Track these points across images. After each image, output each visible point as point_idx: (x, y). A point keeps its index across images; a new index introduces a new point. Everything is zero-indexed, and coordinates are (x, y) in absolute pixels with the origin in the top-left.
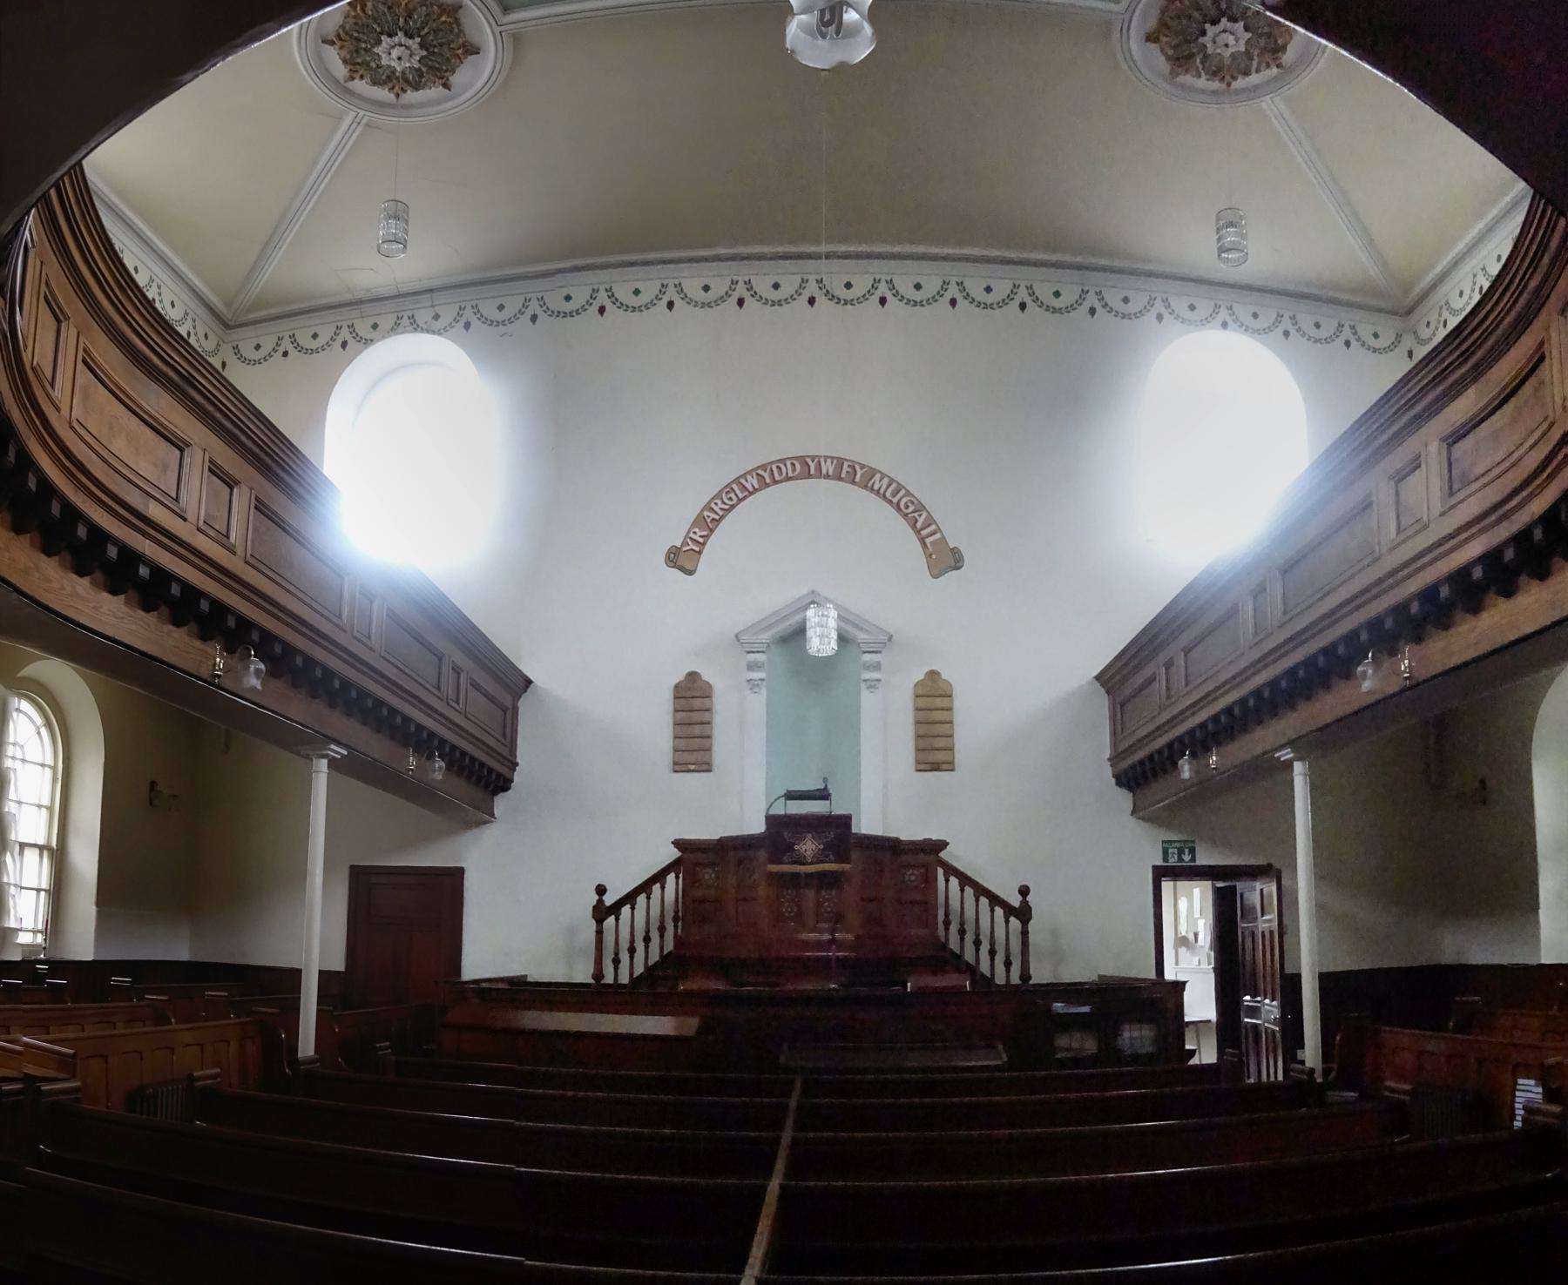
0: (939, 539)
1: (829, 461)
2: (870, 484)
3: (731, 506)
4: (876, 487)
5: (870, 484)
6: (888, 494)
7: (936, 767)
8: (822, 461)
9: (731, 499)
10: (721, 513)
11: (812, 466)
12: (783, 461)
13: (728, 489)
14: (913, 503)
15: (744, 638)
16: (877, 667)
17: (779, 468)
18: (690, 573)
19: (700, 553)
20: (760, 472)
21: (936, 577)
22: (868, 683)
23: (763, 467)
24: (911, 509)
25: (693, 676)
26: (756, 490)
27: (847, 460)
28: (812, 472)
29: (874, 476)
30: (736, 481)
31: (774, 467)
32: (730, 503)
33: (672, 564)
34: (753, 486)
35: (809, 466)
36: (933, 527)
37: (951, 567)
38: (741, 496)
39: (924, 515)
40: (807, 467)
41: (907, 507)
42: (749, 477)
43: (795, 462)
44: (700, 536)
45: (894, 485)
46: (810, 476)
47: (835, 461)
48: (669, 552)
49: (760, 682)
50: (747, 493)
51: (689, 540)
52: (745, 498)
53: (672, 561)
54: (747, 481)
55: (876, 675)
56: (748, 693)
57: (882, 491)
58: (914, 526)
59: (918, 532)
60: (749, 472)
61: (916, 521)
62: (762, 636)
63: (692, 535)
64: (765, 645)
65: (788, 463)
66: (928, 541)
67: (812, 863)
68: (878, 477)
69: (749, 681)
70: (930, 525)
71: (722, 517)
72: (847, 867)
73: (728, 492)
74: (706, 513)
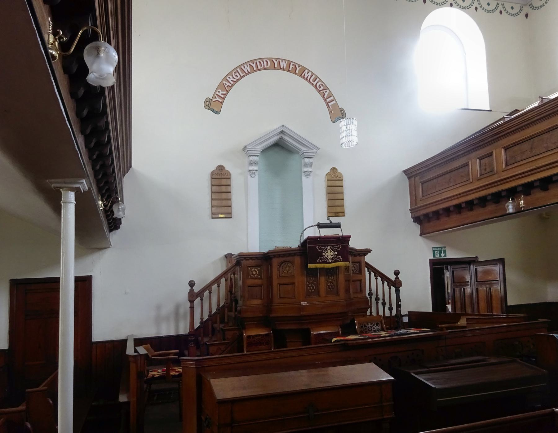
0: (335, 103)
1: (284, 61)
2: (303, 75)
3: (237, 80)
4: (306, 77)
5: (303, 75)
6: (311, 80)
8: (281, 61)
9: (237, 76)
10: (232, 83)
11: (276, 63)
13: (235, 70)
14: (323, 85)
15: (250, 148)
16: (311, 165)
18: (218, 113)
19: (222, 103)
20: (251, 63)
21: (334, 122)
22: (306, 173)
23: (253, 61)
24: (322, 88)
25: (221, 168)
26: (249, 73)
28: (276, 66)
32: (237, 78)
33: (208, 108)
36: (332, 98)
37: (340, 117)
38: (242, 75)
39: (328, 91)
41: (320, 87)
42: (245, 66)
44: (222, 94)
45: (314, 76)
46: (275, 68)
48: (206, 101)
49: (255, 171)
50: (245, 74)
52: (244, 76)
53: (208, 106)
54: (244, 67)
56: (249, 177)
57: (308, 79)
58: (323, 97)
59: (325, 100)
61: (324, 94)
62: (258, 147)
63: (217, 93)
64: (260, 152)
65: (264, 60)
66: (330, 104)
67: (331, 263)
68: (306, 71)
69: (250, 171)
70: (331, 97)
71: (233, 85)
72: (347, 263)
74: (224, 82)
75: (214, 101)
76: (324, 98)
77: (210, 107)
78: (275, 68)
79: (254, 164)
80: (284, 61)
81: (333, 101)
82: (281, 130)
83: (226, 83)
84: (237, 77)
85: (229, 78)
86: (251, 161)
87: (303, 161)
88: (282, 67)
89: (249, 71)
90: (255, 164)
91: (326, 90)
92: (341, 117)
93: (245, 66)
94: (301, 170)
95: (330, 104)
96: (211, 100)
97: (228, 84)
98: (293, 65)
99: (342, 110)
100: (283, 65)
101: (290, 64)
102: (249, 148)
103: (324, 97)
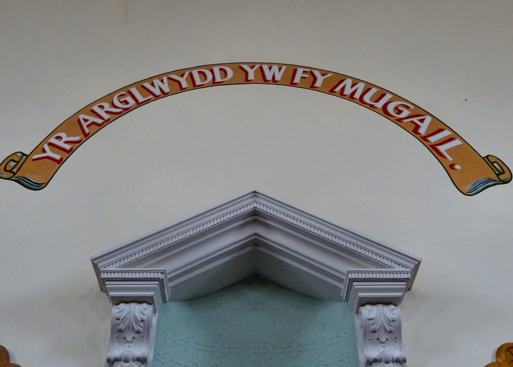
2: (338, 89)
3: (125, 109)
4: (348, 91)
5: (338, 89)
6: (367, 98)
8: (266, 68)
10: (106, 116)
14: (407, 107)
18: (37, 187)
19: (60, 162)
24: (405, 113)
36: (446, 133)
37: (490, 180)
39: (428, 119)
40: (244, 73)
42: (157, 82)
44: (66, 142)
45: (373, 91)
47: (284, 68)
50: (152, 96)
53: (10, 171)
54: (153, 85)
57: (357, 96)
60: (160, 77)
61: (417, 127)
63: (53, 140)
65: (216, 70)
68: (348, 82)
71: (107, 122)
74: (82, 117)
75: (34, 160)
76: (418, 136)
77: (14, 174)
79: (133, 335)
81: (451, 139)
82: (250, 208)
83: (86, 117)
86: (118, 319)
87: (357, 322)
90: (138, 332)
94: (356, 358)
95: (442, 148)
97: (92, 119)
98: (304, 72)
101: (295, 71)
102: (111, 268)
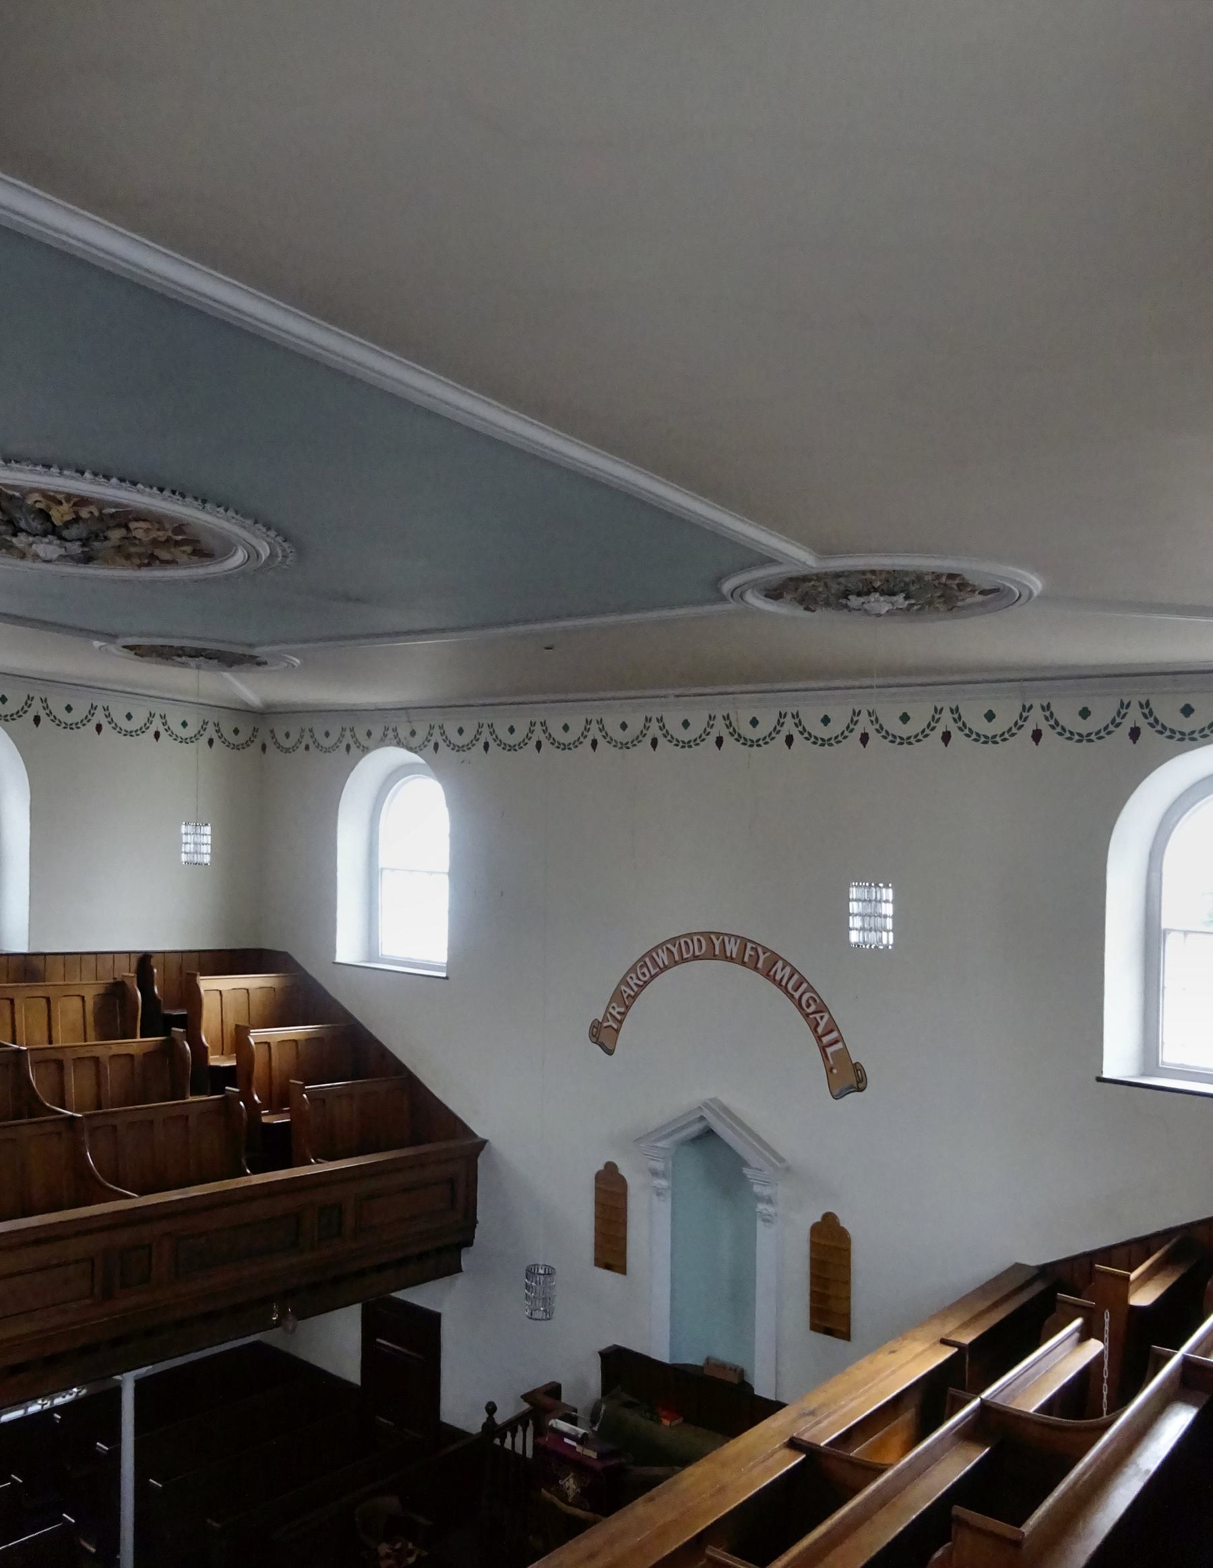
1: (733, 940)
3: (645, 982)
4: (778, 977)
5: (772, 973)
7: (828, 1332)
8: (726, 939)
10: (635, 989)
11: (717, 943)
12: (690, 935)
14: (815, 1001)
16: (769, 1201)
17: (686, 943)
19: (617, 1031)
20: (669, 946)
23: (673, 940)
26: (666, 968)
27: (750, 941)
28: (717, 952)
29: (777, 962)
30: (649, 954)
31: (682, 941)
33: (594, 1040)
34: (663, 962)
35: (714, 945)
36: (834, 1035)
39: (826, 1016)
41: (809, 1006)
42: (660, 951)
43: (702, 939)
45: (796, 977)
46: (715, 957)
47: (738, 941)
48: (593, 1027)
50: (658, 969)
51: (608, 1015)
52: (656, 975)
53: (595, 1036)
55: (771, 1210)
56: (655, 1198)
57: (784, 983)
58: (815, 1030)
59: (819, 1038)
61: (818, 1024)
65: (695, 938)
66: (829, 1050)
68: (780, 964)
70: (831, 1031)
71: (637, 994)
73: (641, 967)
74: (623, 988)
75: (606, 1027)
77: (598, 1039)
78: (715, 955)
80: (733, 940)
81: (836, 1042)
84: (645, 976)
85: (631, 978)
88: (729, 955)
89: (666, 963)
91: (821, 1014)
92: (856, 1085)
93: (660, 951)
95: (829, 1050)
96: (601, 1023)
98: (752, 948)
99: (857, 1068)
100: (732, 948)
103: (816, 1032)
